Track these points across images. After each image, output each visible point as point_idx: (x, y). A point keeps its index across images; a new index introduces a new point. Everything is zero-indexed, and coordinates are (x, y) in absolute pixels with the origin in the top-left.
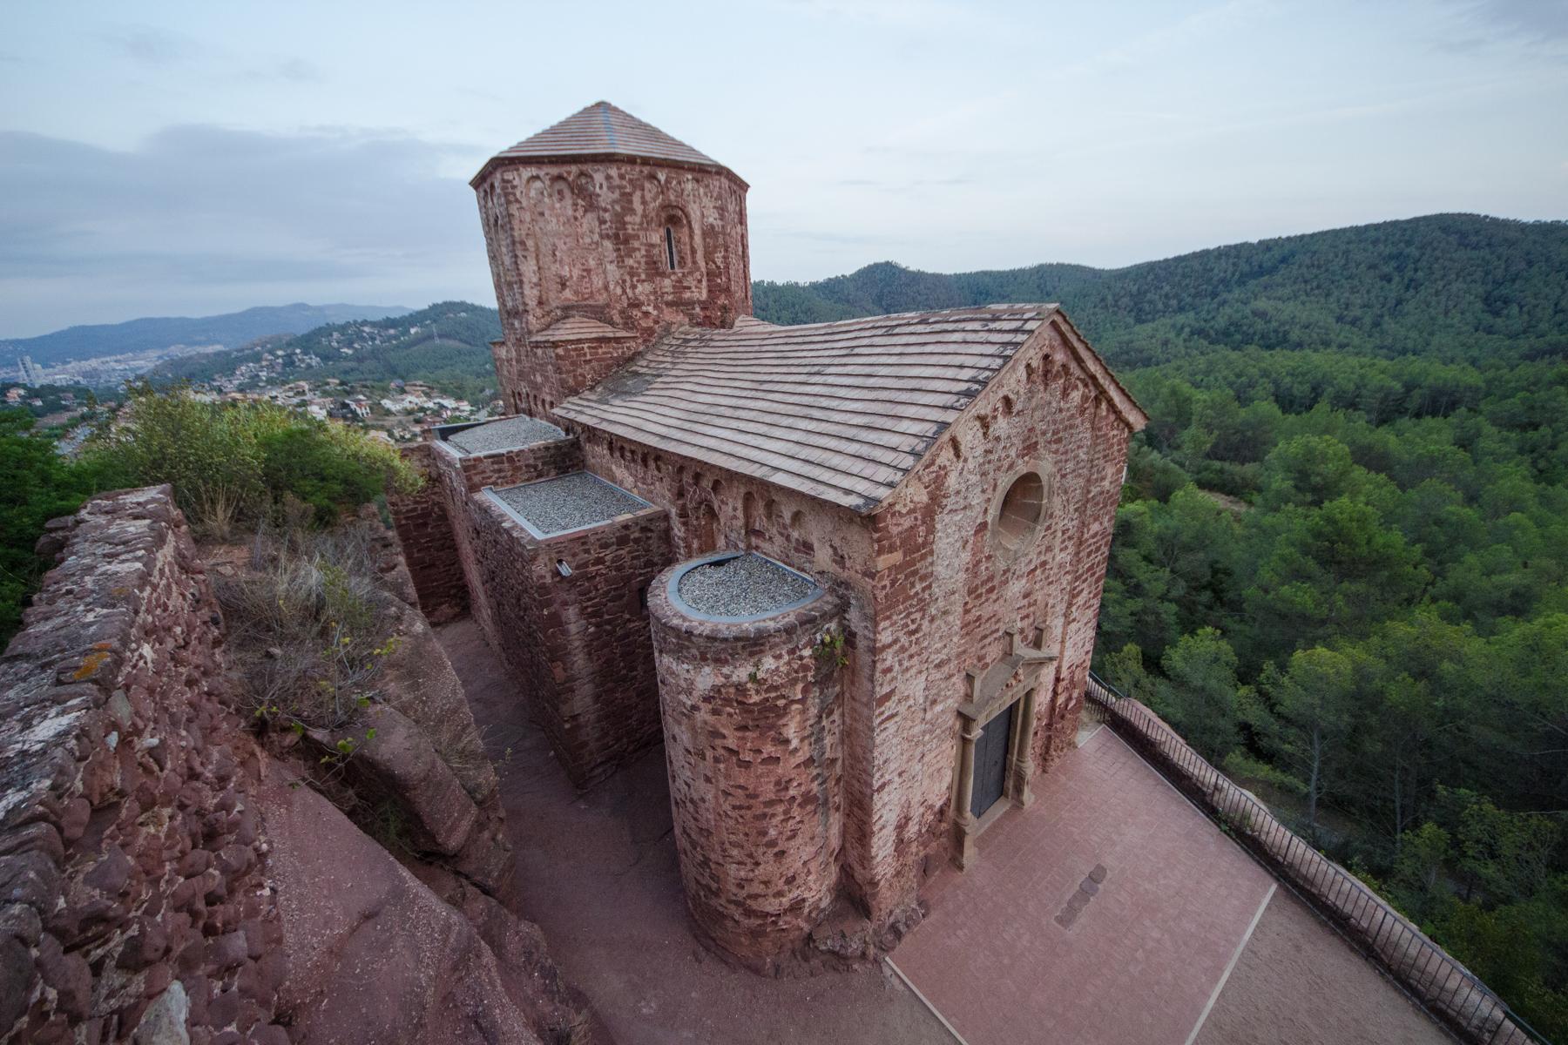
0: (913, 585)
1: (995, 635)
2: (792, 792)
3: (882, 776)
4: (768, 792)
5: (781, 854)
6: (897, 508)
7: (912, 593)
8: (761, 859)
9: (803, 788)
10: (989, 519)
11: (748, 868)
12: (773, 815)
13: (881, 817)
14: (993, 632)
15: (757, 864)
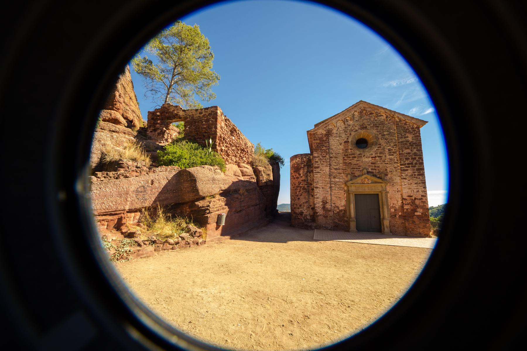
0: (323, 147)
1: (358, 169)
2: (301, 185)
3: (317, 185)
4: (297, 185)
5: (299, 199)
6: (317, 133)
7: (323, 149)
8: (296, 199)
9: (303, 185)
10: (350, 140)
11: (294, 201)
12: (298, 189)
13: (317, 195)
14: (357, 168)
15: (295, 200)
